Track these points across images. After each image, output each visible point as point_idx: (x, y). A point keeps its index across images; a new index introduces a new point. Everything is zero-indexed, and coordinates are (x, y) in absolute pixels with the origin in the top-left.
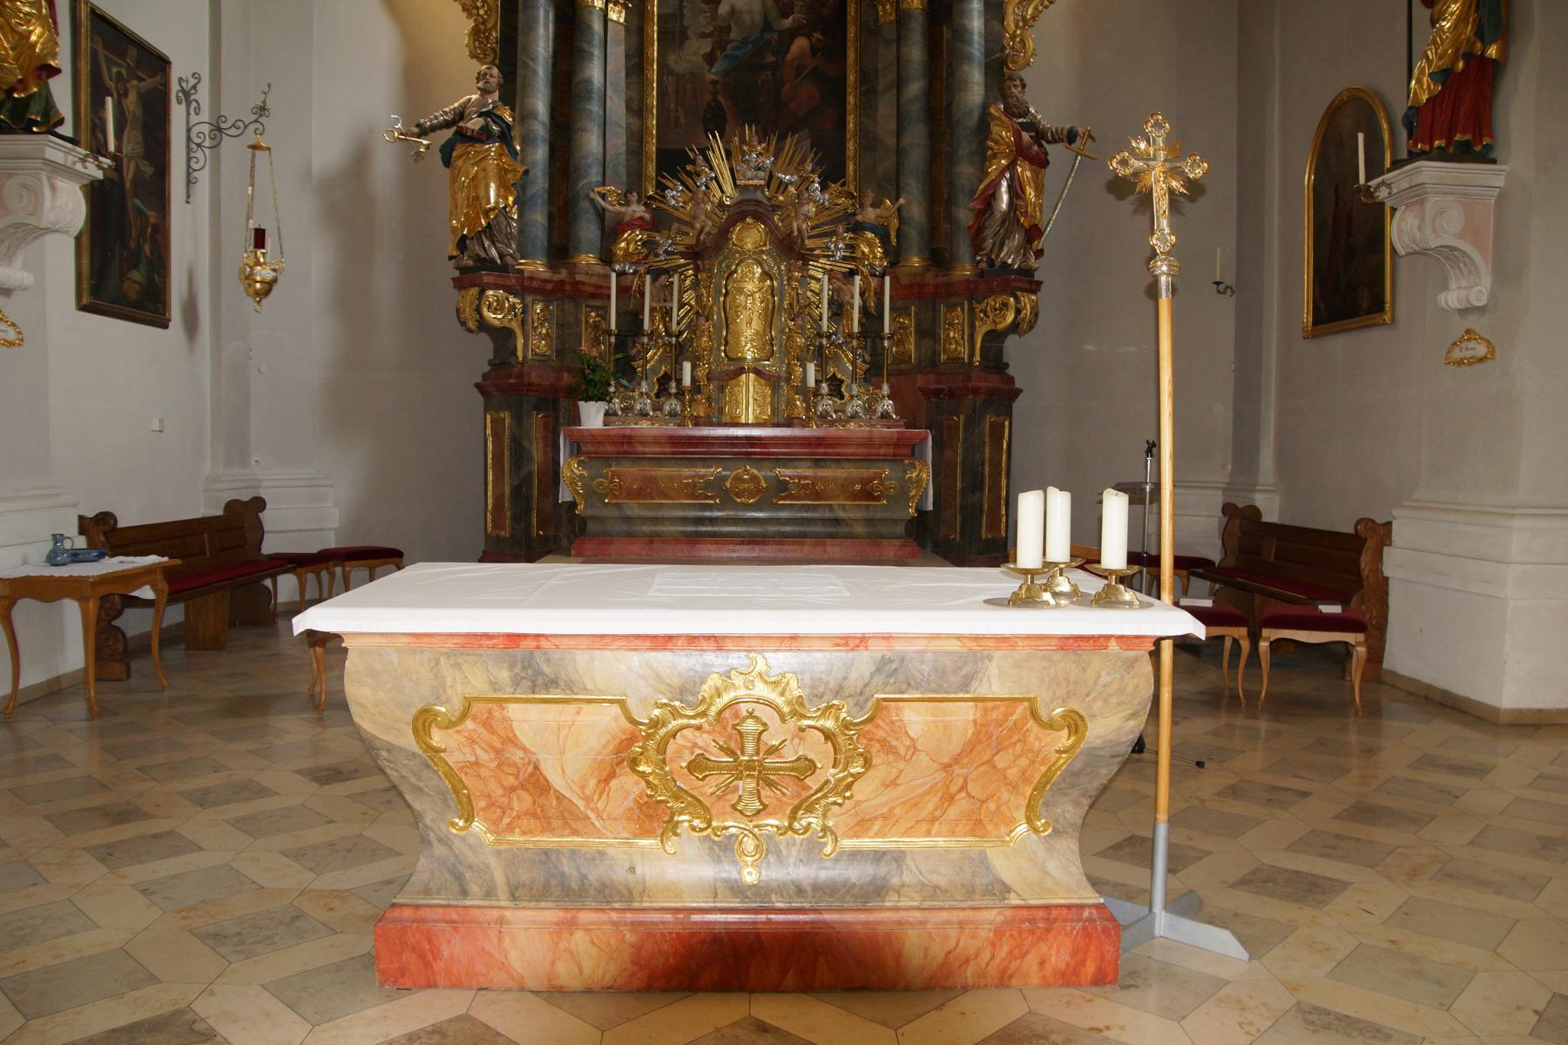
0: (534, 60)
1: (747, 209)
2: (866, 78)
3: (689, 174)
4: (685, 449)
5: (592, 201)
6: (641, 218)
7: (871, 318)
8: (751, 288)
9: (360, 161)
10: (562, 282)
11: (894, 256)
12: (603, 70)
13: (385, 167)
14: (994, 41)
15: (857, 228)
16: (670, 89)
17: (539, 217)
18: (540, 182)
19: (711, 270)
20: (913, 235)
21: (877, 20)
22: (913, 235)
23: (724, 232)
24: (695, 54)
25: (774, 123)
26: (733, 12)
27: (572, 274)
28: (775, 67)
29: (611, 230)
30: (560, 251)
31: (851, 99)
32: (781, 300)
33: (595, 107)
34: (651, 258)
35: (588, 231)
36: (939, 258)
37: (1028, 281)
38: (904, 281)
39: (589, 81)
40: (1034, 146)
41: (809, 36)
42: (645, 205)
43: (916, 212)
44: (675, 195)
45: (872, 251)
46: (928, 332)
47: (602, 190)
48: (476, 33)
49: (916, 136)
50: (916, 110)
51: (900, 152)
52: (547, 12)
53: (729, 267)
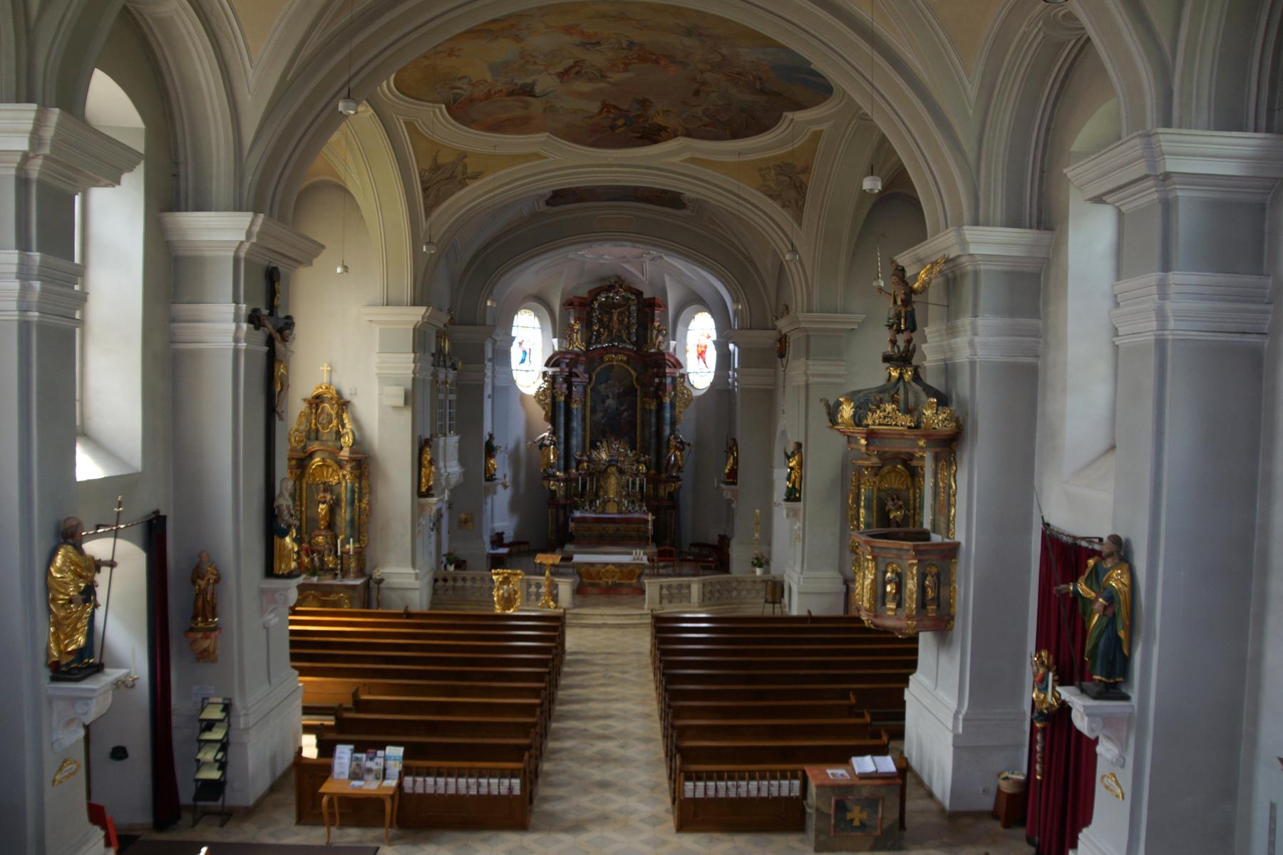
1: (610, 463)
2: (642, 422)
7: (641, 487)
8: (613, 481)
9: (517, 447)
12: (575, 424)
13: (522, 447)
14: (673, 417)
15: (639, 463)
17: (562, 462)
23: (606, 470)
29: (579, 462)
30: (566, 468)
35: (574, 464)
37: (678, 479)
40: (682, 446)
43: (654, 460)
44: (594, 454)
46: (656, 489)
47: (576, 453)
49: (653, 441)
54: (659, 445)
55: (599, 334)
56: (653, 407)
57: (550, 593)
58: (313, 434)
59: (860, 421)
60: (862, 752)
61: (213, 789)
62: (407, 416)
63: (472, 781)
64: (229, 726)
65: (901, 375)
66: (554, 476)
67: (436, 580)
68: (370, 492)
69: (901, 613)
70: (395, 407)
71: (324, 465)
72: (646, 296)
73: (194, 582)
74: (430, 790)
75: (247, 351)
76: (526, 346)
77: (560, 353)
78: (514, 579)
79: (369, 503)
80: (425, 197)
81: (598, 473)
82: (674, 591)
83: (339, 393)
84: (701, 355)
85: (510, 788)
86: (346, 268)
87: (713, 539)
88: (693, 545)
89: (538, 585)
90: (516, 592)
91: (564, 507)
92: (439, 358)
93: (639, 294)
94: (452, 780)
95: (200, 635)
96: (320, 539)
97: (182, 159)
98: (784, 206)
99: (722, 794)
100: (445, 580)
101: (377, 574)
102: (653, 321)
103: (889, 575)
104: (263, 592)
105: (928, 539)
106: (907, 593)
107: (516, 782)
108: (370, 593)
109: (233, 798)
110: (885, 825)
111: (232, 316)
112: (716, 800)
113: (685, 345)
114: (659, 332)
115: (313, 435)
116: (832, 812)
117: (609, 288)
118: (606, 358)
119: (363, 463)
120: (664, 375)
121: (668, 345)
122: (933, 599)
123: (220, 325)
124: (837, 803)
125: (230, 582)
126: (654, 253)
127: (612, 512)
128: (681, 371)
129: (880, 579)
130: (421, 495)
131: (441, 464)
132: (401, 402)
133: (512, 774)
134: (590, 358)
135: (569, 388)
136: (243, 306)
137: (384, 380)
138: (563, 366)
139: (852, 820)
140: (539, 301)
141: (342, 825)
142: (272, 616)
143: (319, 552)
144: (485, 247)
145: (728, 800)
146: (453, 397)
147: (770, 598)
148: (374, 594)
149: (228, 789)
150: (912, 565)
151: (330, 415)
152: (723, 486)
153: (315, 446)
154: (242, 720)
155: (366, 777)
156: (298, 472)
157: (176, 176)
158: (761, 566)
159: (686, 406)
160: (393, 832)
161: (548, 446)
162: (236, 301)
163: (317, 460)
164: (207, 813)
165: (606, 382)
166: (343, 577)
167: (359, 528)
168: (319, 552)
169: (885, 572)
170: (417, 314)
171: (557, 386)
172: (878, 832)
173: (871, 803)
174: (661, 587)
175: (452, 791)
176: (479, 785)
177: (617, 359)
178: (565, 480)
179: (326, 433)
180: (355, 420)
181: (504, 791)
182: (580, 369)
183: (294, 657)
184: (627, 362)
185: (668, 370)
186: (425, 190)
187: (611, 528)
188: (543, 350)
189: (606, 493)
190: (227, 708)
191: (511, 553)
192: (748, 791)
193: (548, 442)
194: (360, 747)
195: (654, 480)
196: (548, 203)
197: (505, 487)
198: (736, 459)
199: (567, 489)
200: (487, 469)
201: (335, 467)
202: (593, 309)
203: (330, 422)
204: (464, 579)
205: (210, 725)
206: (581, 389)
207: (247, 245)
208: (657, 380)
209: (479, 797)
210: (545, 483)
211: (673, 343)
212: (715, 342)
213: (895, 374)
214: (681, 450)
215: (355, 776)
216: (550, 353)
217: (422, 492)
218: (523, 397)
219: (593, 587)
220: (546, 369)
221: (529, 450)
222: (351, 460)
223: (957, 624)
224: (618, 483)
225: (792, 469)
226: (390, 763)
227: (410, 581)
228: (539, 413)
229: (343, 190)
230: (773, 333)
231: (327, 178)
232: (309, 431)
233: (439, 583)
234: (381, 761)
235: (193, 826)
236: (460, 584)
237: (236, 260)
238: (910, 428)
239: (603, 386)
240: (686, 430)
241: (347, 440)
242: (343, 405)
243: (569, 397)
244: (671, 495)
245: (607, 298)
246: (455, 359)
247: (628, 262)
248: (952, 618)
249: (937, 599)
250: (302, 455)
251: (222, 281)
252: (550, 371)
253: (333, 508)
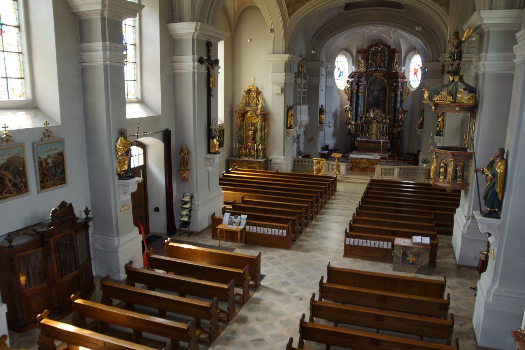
1: (374, 118)
2: (389, 102)
4: (367, 142)
7: (386, 129)
8: (374, 125)
9: (336, 111)
15: (386, 119)
17: (354, 118)
18: (354, 114)
25: (378, 107)
29: (361, 118)
30: (356, 120)
35: (359, 118)
36: (394, 122)
37: (402, 126)
40: (404, 112)
43: (392, 117)
44: (368, 115)
46: (393, 130)
47: (360, 114)
48: (348, 98)
49: (393, 110)
54: (395, 111)
55: (371, 65)
56: (393, 95)
57: (337, 168)
58: (248, 104)
59: (432, 99)
60: (417, 235)
61: (186, 224)
62: (282, 97)
63: (269, 229)
64: (192, 204)
65: (453, 79)
66: (350, 123)
67: (295, 162)
68: (268, 127)
69: (446, 181)
70: (278, 94)
71: (252, 116)
72: (392, 48)
73: (180, 154)
74: (255, 231)
75: (198, 73)
76: (341, 70)
77: (355, 72)
78: (321, 162)
79: (268, 131)
80: (288, 10)
81: (369, 123)
82: (387, 171)
83: (257, 88)
84: (415, 73)
85: (282, 233)
86: (251, 40)
87: (415, 152)
88: (407, 154)
89: (333, 165)
90: (322, 167)
91: (354, 136)
92: (298, 75)
93: (389, 47)
94: (262, 228)
95: (182, 172)
96: (250, 144)
97: (174, 4)
98: (441, 5)
99: (360, 244)
100: (298, 162)
101: (270, 158)
102: (394, 58)
103: (442, 164)
104: (206, 158)
105: (467, 151)
106: (448, 172)
107: (285, 231)
108: (267, 164)
109: (192, 228)
110: (422, 265)
111: (192, 60)
112: (358, 246)
113: (409, 69)
114: (397, 63)
115: (248, 105)
116: (401, 256)
117: (376, 45)
118: (374, 75)
119: (265, 116)
120: (398, 82)
121: (401, 70)
122: (460, 176)
123: (188, 63)
124: (403, 253)
125: (193, 155)
126: (393, 29)
127: (374, 138)
128: (406, 80)
129: (438, 166)
130: (288, 128)
131: (298, 117)
132: (280, 92)
133: (283, 228)
134: (368, 75)
135: (358, 87)
136: (196, 56)
137: (273, 83)
138: (356, 78)
139: (409, 260)
140: (347, 50)
141: (226, 241)
142: (210, 167)
143: (249, 149)
144: (320, 29)
145: (362, 247)
146: (305, 90)
147: (427, 176)
148: (269, 165)
149: (191, 225)
150: (452, 161)
151: (254, 97)
152: (417, 129)
153: (248, 109)
154: (196, 202)
155: (234, 224)
156: (242, 118)
157: (172, 10)
158: (426, 163)
159: (407, 95)
160: (240, 244)
161: (348, 111)
162: (193, 54)
163: (249, 114)
164: (185, 232)
166: (257, 158)
167: (264, 140)
168: (249, 149)
169: (441, 163)
170: (286, 57)
171: (353, 86)
172: (419, 267)
173: (417, 255)
174: (382, 169)
175: (262, 232)
176: (272, 231)
177: (379, 75)
178: (355, 125)
179: (252, 104)
180: (263, 99)
181: (280, 234)
182: (364, 79)
183: (220, 184)
184: (383, 76)
185: (399, 80)
186: (288, 7)
187: (372, 145)
188: (348, 72)
189: (371, 131)
190: (192, 198)
191: (326, 154)
192: (370, 244)
193: (348, 109)
194: (232, 214)
195: (392, 126)
196: (345, 9)
197: (330, 127)
198: (423, 118)
199: (356, 129)
200: (320, 119)
201: (256, 117)
202: (369, 54)
203: (254, 100)
204: (305, 162)
205: (186, 203)
206: (363, 87)
207: (196, 34)
208: (395, 84)
209: (271, 235)
210: (347, 126)
211: (403, 68)
212: (420, 68)
213: (451, 79)
214: (404, 114)
215: (230, 224)
216: (351, 72)
217: (288, 127)
218: (339, 90)
219: (355, 168)
220: (349, 79)
221: (341, 112)
222: (261, 114)
223: (470, 187)
224: (377, 127)
225: (439, 122)
226: (242, 220)
227: (283, 161)
228: (345, 97)
229: (257, 8)
230: (440, 64)
231: (251, 4)
232: (246, 103)
233: (296, 162)
234: (239, 219)
235: (180, 235)
236: (304, 163)
237: (193, 40)
238: (452, 102)
239: (373, 86)
240: (407, 106)
241: (260, 107)
242: (258, 93)
243: (358, 91)
244: (399, 133)
245: (375, 49)
246: (305, 76)
247: (383, 33)
248: (468, 185)
249: (462, 177)
250: (243, 112)
251: (188, 47)
252: (351, 80)
253: (255, 133)
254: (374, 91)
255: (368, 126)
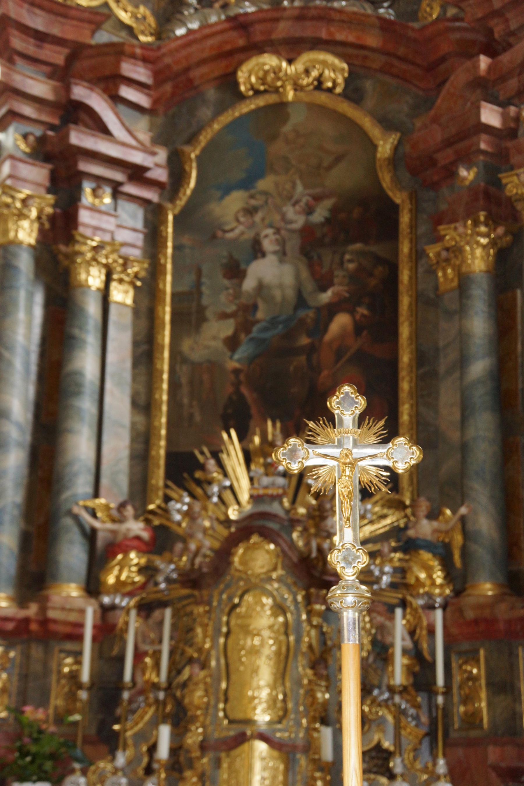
0: (10, 348)
2: (423, 359)
3: (199, 483)
5: (76, 518)
6: (138, 538)
7: (421, 664)
10: (26, 621)
11: (459, 580)
15: (410, 546)
16: (184, 380)
19: (209, 603)
20: (482, 554)
21: (437, 288)
22: (482, 554)
23: (223, 555)
24: (214, 338)
26: (261, 287)
27: (43, 609)
28: (311, 350)
31: (405, 386)
32: (298, 640)
33: (87, 405)
34: (150, 587)
35: (73, 555)
38: (470, 615)
39: (80, 373)
41: (352, 312)
42: (147, 521)
44: (181, 504)
45: (430, 576)
50: (481, 395)
51: (464, 448)
52: (30, 296)
53: (230, 598)
118: (247, 75)
165: (246, 184)
182: (125, 136)
184: (353, 92)
206: (132, 216)
208: (490, 116)
239: (236, 201)
254: (257, 251)
255: (183, 634)
